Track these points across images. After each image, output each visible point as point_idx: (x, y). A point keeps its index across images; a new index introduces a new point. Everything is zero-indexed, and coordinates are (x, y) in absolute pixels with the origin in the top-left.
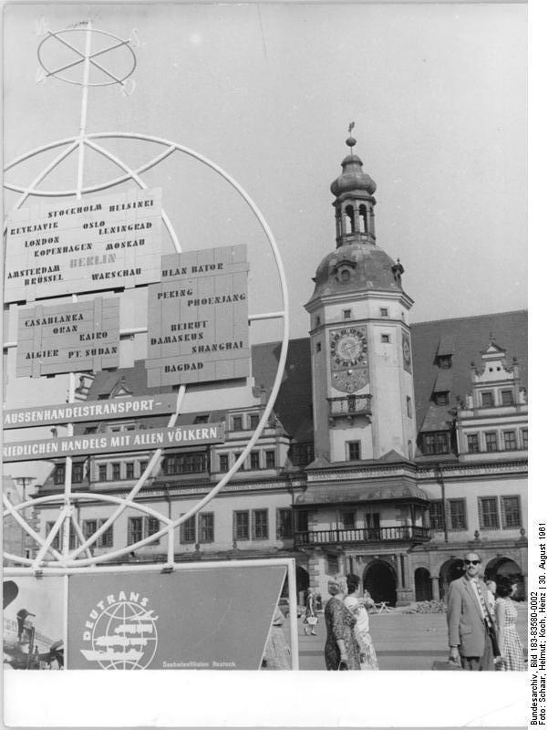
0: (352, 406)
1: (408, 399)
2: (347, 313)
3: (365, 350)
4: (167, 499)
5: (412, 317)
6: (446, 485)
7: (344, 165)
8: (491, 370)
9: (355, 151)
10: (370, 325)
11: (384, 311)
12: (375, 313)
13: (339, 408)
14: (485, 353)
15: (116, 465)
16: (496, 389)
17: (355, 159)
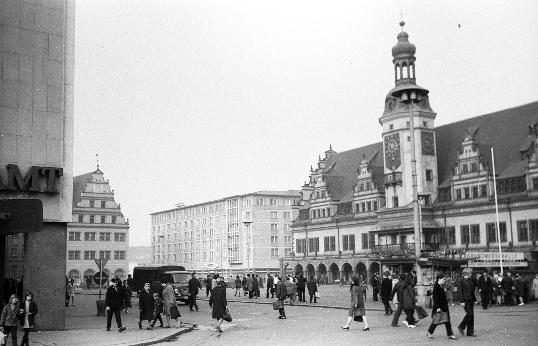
0: (394, 178)
1: (428, 172)
2: (391, 126)
3: (399, 147)
4: (338, 227)
5: (437, 123)
6: (448, 219)
7: (398, 38)
8: (467, 151)
9: (405, 29)
10: (400, 132)
12: (405, 126)
13: (390, 179)
14: (463, 141)
15: (319, 211)
16: (469, 163)
17: (402, 35)
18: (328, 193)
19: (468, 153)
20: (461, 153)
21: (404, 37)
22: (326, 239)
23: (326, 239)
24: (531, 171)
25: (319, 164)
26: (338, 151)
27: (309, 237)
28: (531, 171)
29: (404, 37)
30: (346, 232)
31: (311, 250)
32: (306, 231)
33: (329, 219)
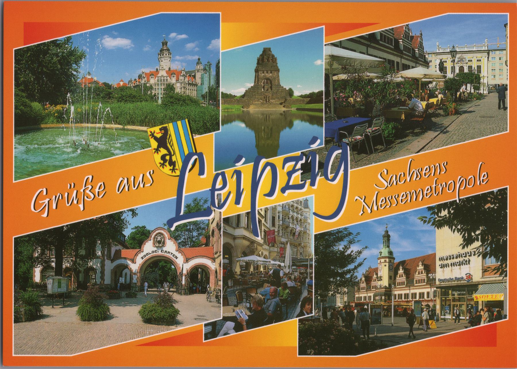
21: (387, 232)
29: (387, 232)
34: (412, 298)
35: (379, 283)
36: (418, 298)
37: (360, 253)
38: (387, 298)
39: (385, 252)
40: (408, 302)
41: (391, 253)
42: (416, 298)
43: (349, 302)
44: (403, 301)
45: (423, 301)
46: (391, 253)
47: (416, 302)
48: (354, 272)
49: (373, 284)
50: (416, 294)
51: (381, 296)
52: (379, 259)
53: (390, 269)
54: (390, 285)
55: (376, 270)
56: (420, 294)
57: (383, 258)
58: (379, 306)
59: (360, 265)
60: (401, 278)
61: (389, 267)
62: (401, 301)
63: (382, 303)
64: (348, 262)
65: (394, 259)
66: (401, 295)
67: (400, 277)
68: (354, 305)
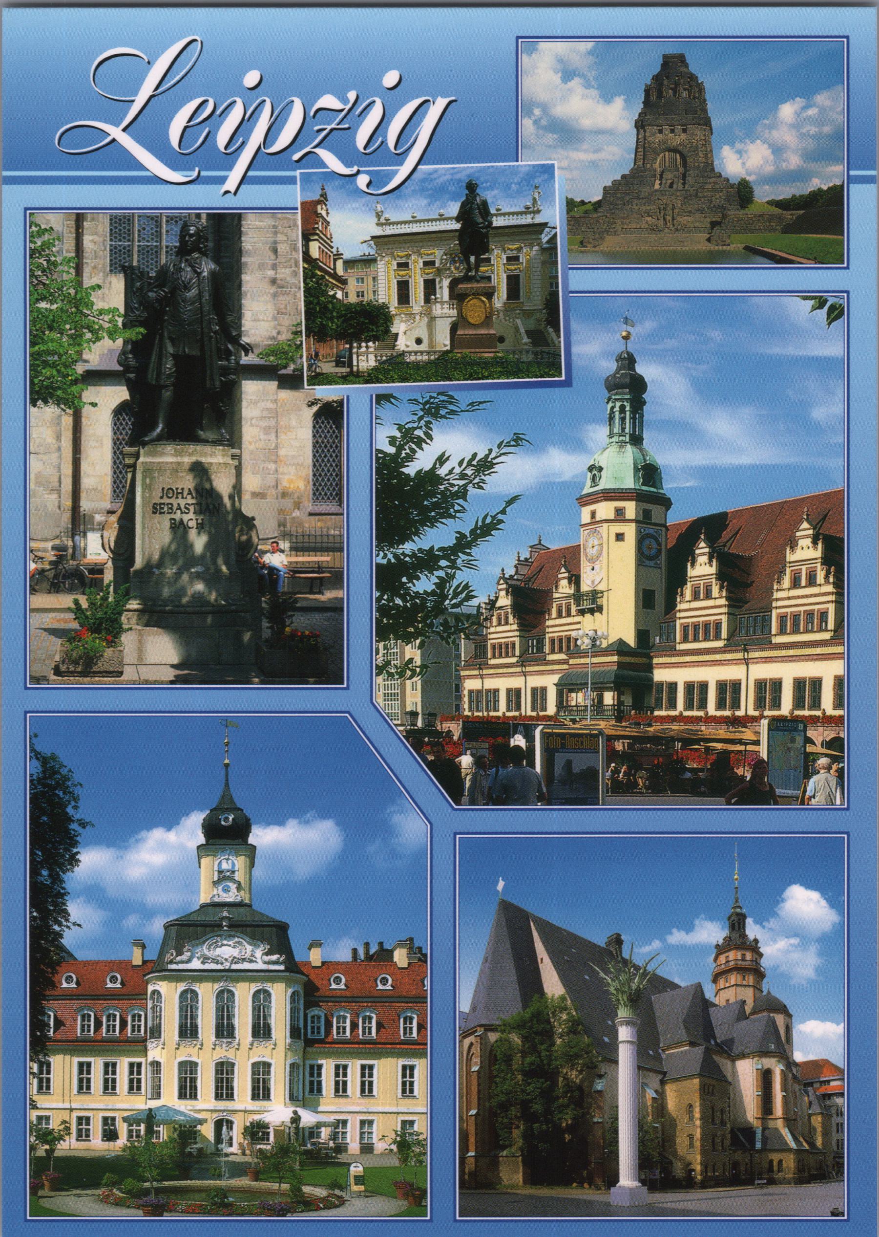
4: (525, 674)
11: (620, 512)
16: (702, 582)
18: (514, 617)
19: (702, 568)
20: (693, 565)
22: (509, 691)
23: (509, 691)
24: (780, 603)
25: (516, 567)
26: (554, 547)
27: (485, 687)
28: (780, 603)
30: (535, 681)
31: (478, 711)
32: (482, 677)
33: (514, 660)
34: (760, 703)
35: (589, 624)
36: (786, 707)
37: (485, 465)
38: (628, 700)
39: (619, 467)
40: (735, 722)
41: (649, 473)
42: (776, 703)
43: (430, 716)
44: (709, 720)
45: (814, 720)
46: (649, 473)
47: (777, 724)
48: (454, 566)
49: (555, 626)
50: (777, 685)
51: (599, 688)
52: (585, 500)
53: (643, 557)
54: (642, 635)
55: (570, 559)
56: (799, 684)
57: (609, 495)
58: (585, 742)
59: (486, 529)
60: (703, 600)
61: (641, 541)
62: (698, 719)
63: (602, 724)
64: (424, 511)
65: (666, 503)
66: (704, 686)
67: (696, 597)
68: (456, 729)
